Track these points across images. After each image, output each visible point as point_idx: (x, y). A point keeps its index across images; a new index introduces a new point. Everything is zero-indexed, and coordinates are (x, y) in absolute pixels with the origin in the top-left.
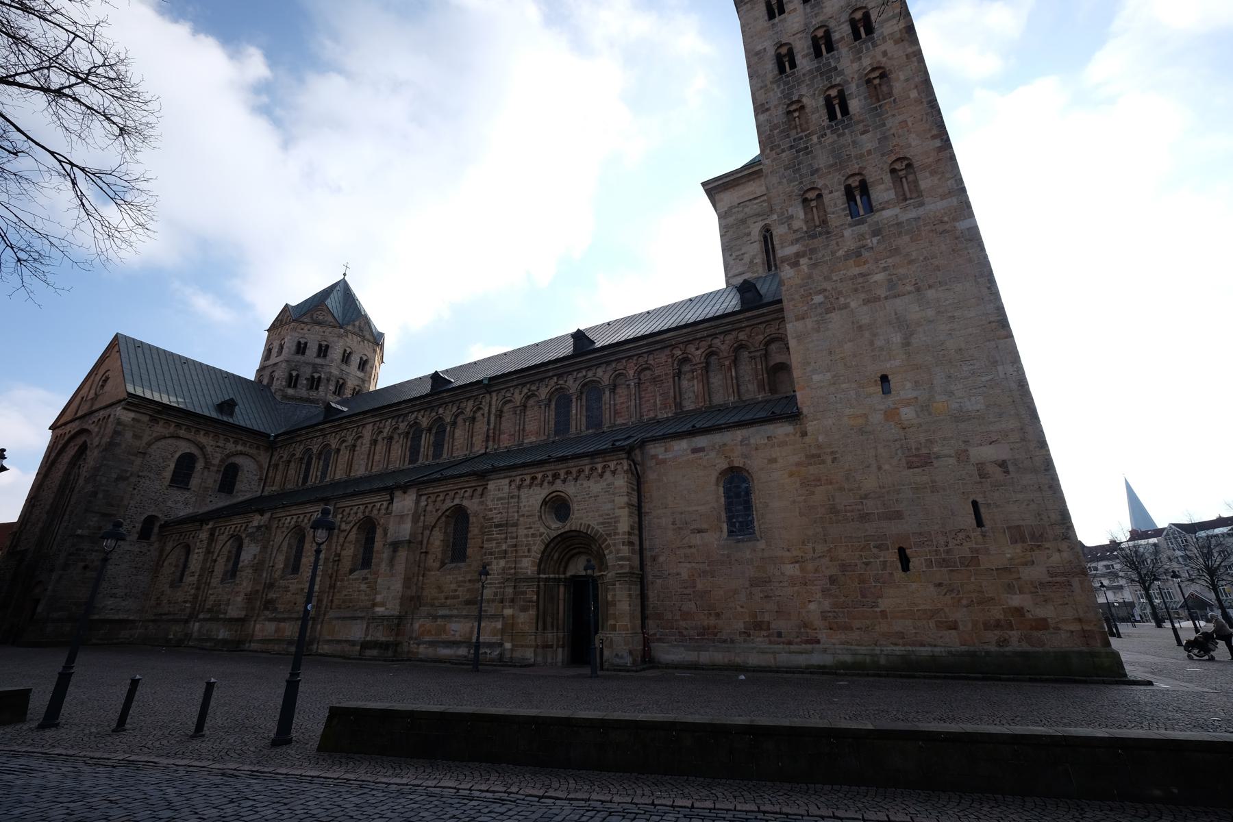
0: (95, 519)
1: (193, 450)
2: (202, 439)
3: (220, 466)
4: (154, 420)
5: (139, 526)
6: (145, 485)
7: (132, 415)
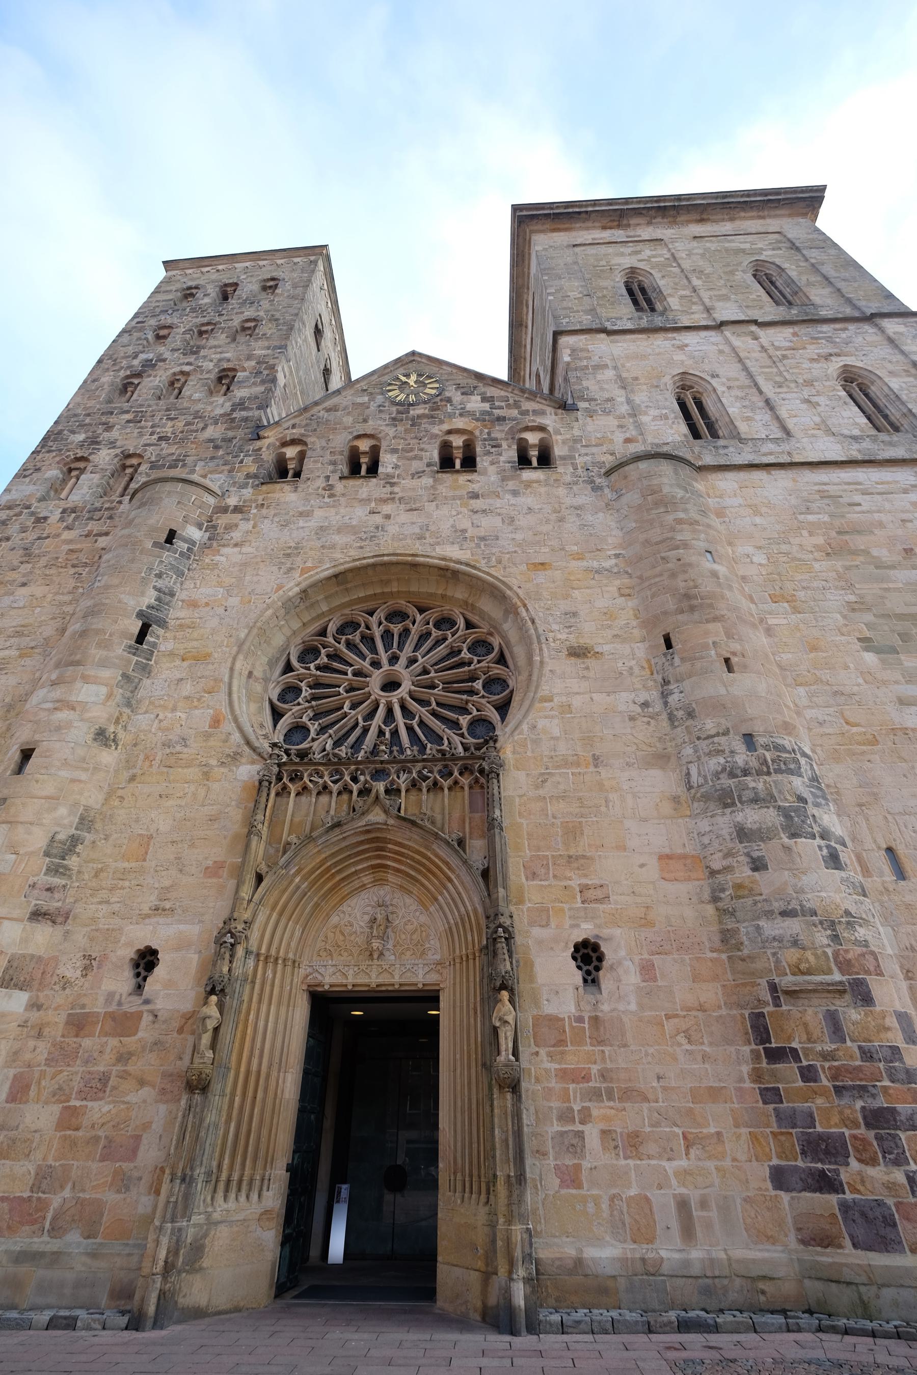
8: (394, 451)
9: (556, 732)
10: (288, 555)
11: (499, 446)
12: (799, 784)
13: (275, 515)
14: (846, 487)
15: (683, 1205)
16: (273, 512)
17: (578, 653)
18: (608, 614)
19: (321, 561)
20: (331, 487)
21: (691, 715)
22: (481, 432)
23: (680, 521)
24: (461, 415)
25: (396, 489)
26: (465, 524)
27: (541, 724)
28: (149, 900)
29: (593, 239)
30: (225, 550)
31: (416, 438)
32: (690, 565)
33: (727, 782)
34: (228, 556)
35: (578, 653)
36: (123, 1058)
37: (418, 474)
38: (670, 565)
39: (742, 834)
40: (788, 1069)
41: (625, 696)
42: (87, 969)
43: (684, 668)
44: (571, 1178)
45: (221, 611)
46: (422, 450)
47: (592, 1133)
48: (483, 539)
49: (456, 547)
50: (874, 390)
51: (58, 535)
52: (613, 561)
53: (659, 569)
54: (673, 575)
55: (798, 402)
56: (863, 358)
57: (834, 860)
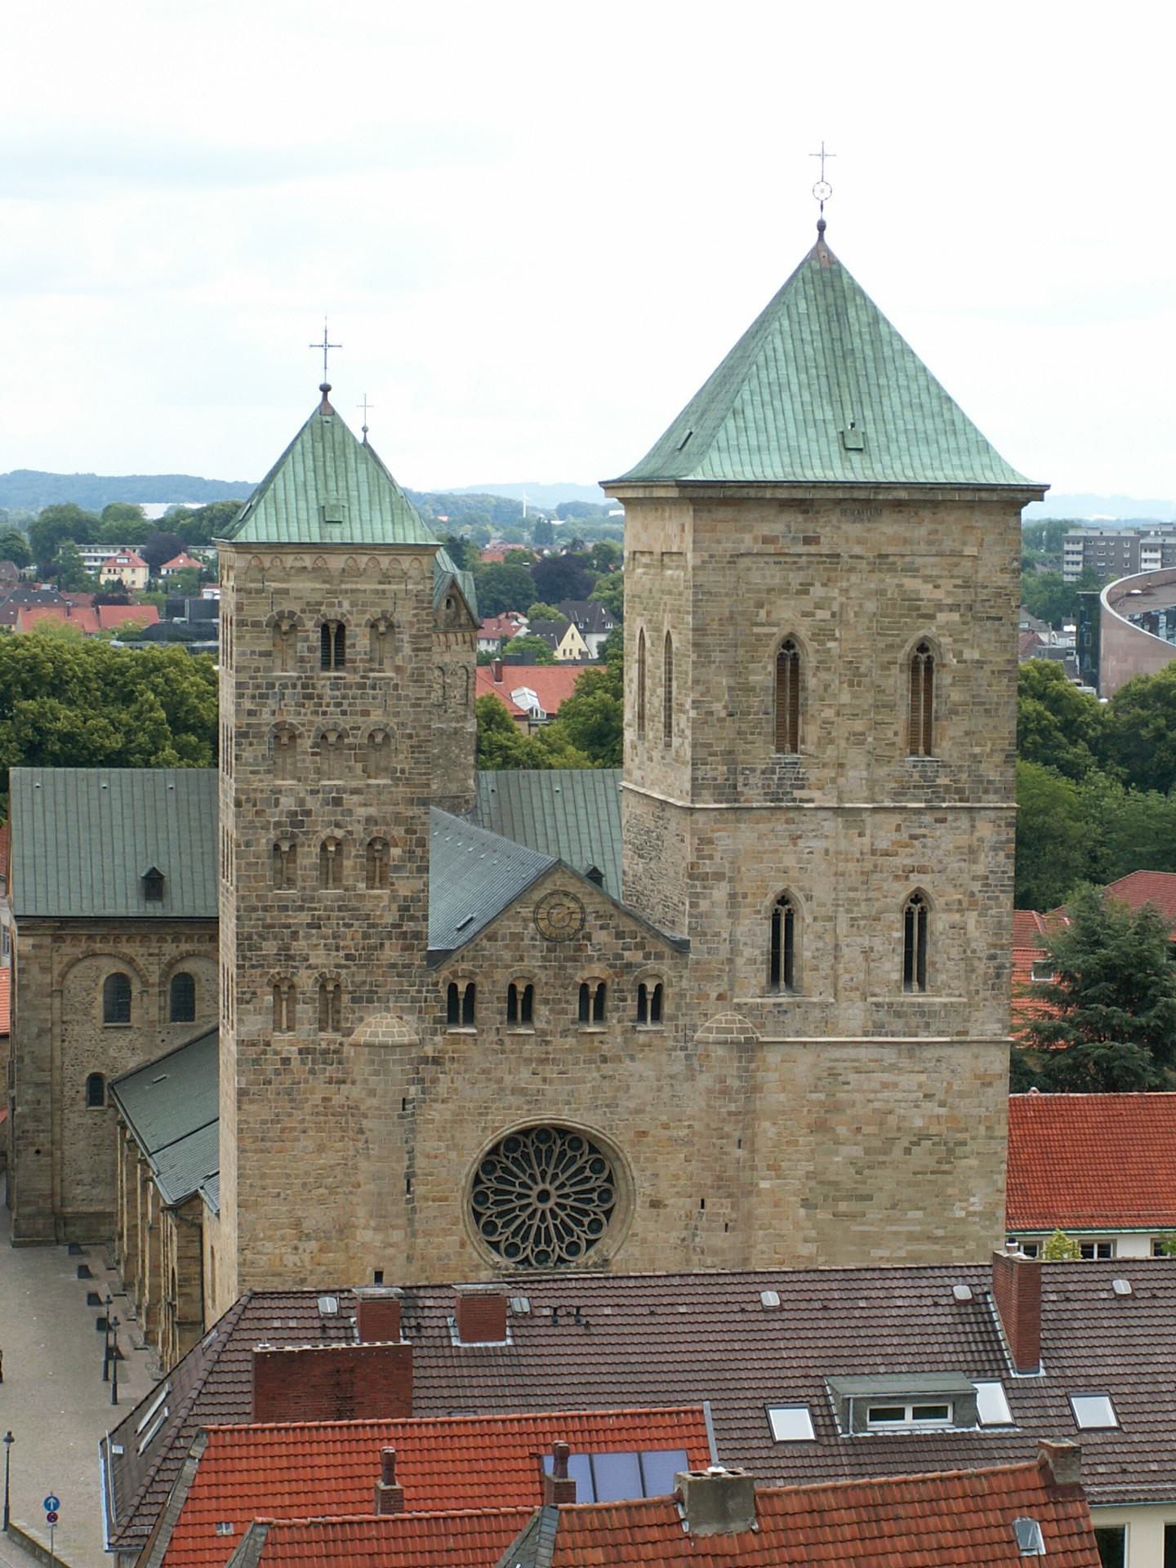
0: (31, 1091)
1: (123, 968)
2: (126, 948)
3: (161, 984)
4: (58, 939)
5: (83, 1090)
6: (75, 1032)
7: (30, 941)
8: (546, 1002)
10: (481, 1114)
11: (624, 1000)
13: (466, 1071)
16: (463, 1068)
17: (655, 1204)
18: (676, 1177)
19: (504, 1121)
20: (501, 1042)
21: (702, 1252)
22: (613, 981)
23: (730, 1113)
24: (599, 959)
25: (550, 1048)
29: (766, 540)
30: (436, 1106)
31: (562, 986)
34: (438, 1113)
35: (655, 1204)
37: (565, 1033)
41: (674, 1234)
45: (445, 1162)
46: (567, 1002)
50: (929, 916)
51: (306, 1081)
52: (686, 1131)
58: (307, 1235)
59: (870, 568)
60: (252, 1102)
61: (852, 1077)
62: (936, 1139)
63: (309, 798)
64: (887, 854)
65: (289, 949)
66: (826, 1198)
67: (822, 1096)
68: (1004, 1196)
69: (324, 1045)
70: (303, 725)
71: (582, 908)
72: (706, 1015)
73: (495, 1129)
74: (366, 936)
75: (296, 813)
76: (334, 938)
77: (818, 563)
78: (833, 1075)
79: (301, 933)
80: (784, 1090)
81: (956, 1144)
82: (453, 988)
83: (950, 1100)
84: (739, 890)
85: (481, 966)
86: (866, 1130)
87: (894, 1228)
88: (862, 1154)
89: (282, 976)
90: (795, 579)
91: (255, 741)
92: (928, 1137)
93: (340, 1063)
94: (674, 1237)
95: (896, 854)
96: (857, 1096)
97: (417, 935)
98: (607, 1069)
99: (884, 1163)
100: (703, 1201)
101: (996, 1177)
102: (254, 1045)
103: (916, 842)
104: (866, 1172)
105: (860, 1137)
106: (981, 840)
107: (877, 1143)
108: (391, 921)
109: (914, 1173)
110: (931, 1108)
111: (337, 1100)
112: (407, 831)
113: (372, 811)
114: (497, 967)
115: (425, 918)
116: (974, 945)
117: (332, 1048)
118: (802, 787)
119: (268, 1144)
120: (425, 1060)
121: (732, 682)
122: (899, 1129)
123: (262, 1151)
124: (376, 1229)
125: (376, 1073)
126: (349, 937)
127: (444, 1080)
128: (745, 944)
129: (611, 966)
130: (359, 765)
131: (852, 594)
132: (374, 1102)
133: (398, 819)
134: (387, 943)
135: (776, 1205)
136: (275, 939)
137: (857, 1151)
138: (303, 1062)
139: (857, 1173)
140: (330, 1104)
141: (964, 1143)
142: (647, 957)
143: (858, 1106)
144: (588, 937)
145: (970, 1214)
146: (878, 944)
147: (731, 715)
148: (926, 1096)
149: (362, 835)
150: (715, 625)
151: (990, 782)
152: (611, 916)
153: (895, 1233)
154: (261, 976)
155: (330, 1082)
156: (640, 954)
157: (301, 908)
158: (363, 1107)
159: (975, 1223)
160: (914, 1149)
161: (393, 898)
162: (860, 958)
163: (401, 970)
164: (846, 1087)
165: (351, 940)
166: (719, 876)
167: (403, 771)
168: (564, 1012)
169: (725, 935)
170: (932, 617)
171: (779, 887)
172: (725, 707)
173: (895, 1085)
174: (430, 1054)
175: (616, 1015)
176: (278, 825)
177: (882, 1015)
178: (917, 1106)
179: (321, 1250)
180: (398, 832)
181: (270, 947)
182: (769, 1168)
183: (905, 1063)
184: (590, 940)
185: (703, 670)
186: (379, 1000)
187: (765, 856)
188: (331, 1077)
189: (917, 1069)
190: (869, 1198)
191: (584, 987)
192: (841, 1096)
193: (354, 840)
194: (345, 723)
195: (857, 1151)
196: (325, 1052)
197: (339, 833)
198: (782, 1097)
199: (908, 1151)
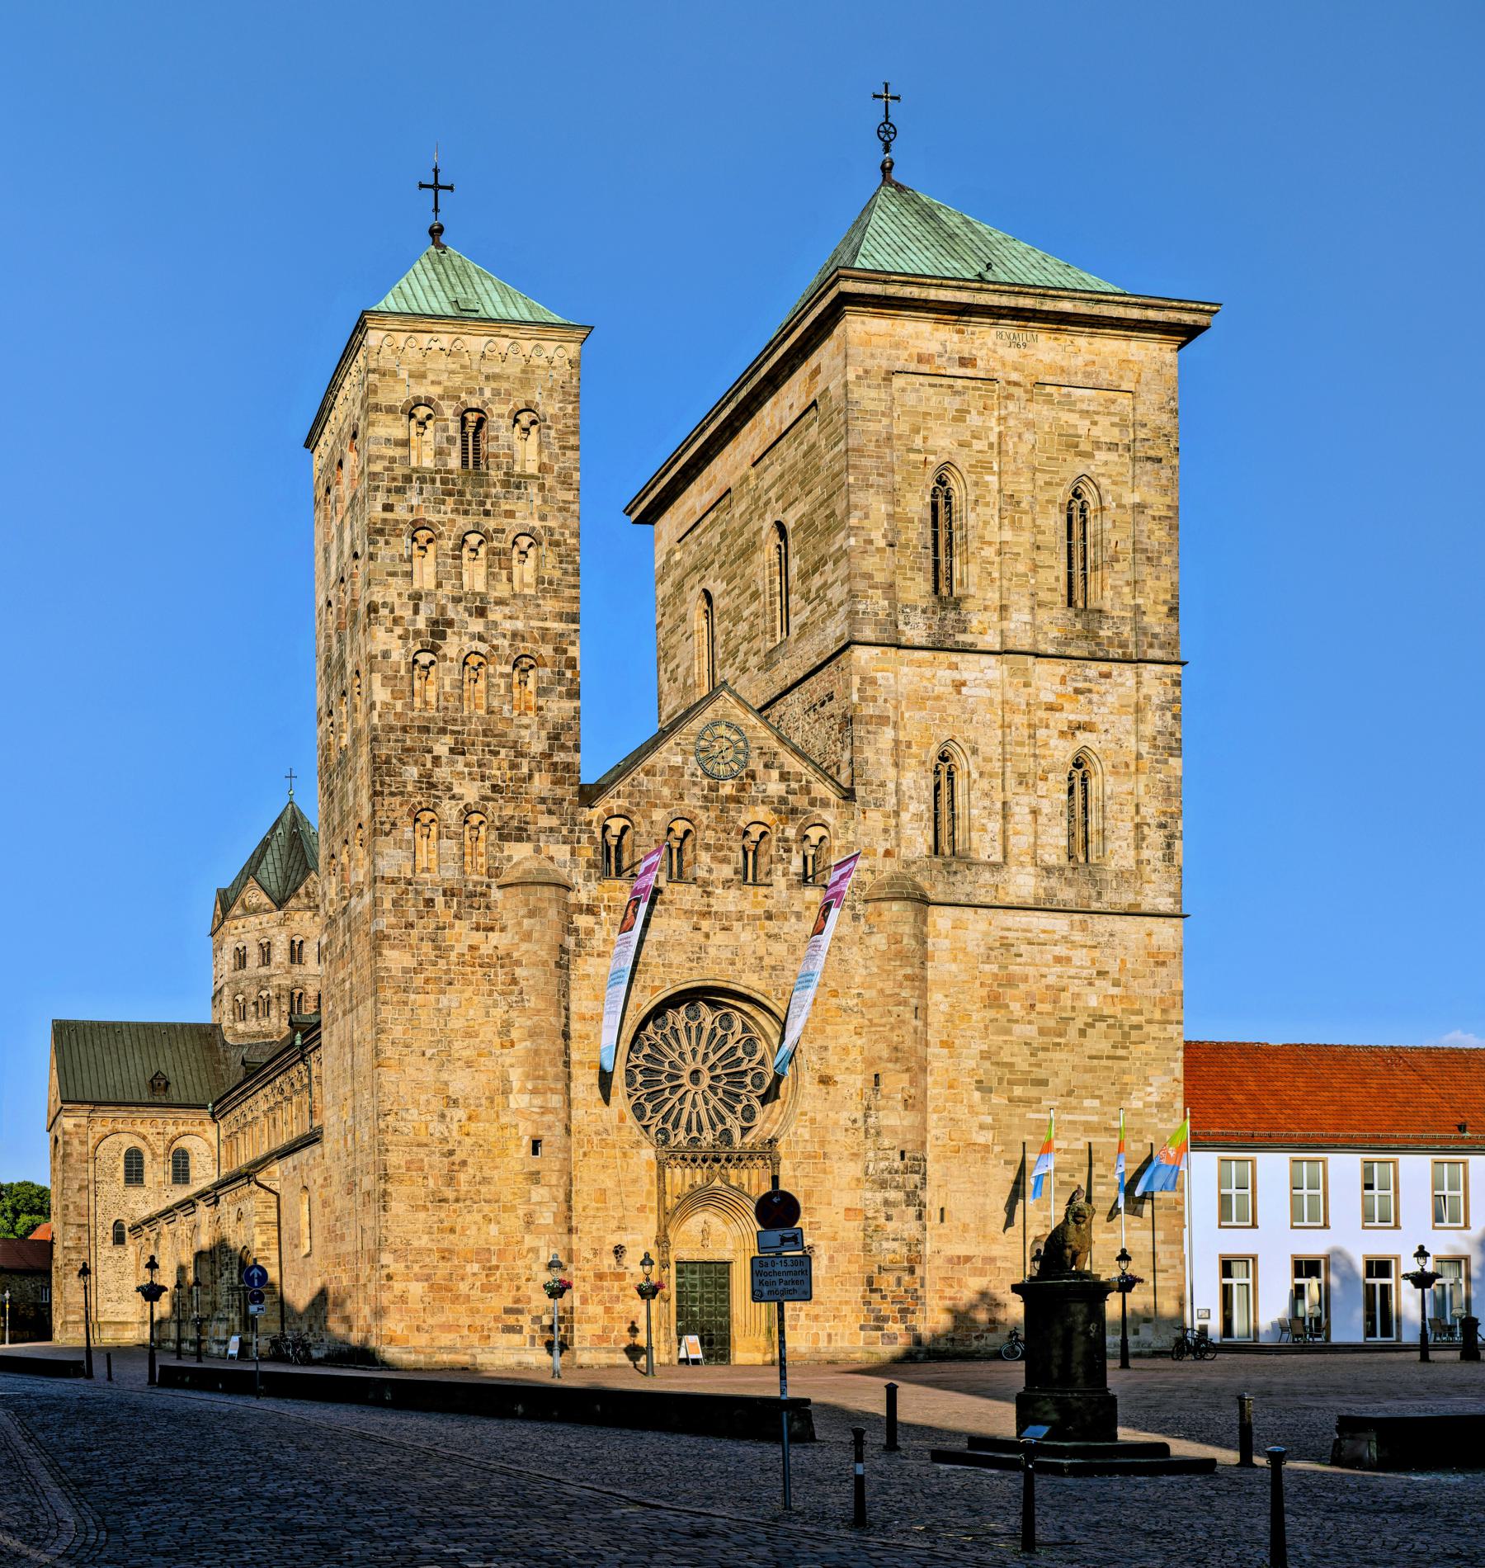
9: (807, 1137)
11: (788, 850)
12: (917, 1177)
14: (1020, 934)
15: (829, 1335)
17: (825, 1080)
18: (845, 1050)
23: (906, 977)
25: (712, 901)
26: (761, 952)
27: (800, 1131)
28: (614, 1224)
30: (591, 960)
31: (724, 831)
32: (903, 1022)
33: (886, 1176)
35: (825, 1080)
36: (622, 1289)
37: (727, 884)
38: (892, 1020)
39: (886, 1203)
40: (876, 1297)
41: (845, 1114)
42: (595, 1254)
43: (882, 1103)
44: (794, 1328)
46: (730, 849)
47: (802, 1314)
48: (774, 968)
49: (756, 976)
51: (452, 926)
52: (855, 1001)
53: (884, 1020)
54: (892, 1029)
55: (1027, 810)
56: (1103, 737)
57: (920, 1217)
58: (455, 1101)
59: (1028, 396)
60: (393, 947)
61: (1024, 948)
62: (1111, 1021)
63: (450, 606)
64: (1051, 708)
65: (431, 776)
66: (1000, 1080)
67: (994, 968)
68: (1181, 1087)
69: (470, 887)
70: (443, 524)
71: (745, 740)
72: (873, 872)
73: (655, 989)
74: (514, 766)
75: (435, 623)
76: (480, 766)
77: (974, 389)
78: (1007, 946)
79: (444, 760)
80: (955, 960)
81: (1133, 1027)
82: (605, 828)
83: (1123, 979)
84: (902, 736)
85: (638, 804)
86: (1039, 1007)
87: (1070, 1117)
88: (1035, 1033)
89: (424, 805)
90: (955, 403)
91: (392, 540)
92: (1102, 1018)
93: (488, 907)
94: (844, 1118)
95: (1062, 709)
96: (1031, 971)
97: (568, 767)
98: (772, 926)
99: (1059, 1044)
100: (877, 1076)
101: (1173, 1065)
102: (393, 882)
103: (1081, 697)
104: (1041, 1054)
105: (1034, 1015)
106: (1148, 698)
107: (1052, 1023)
108: (540, 750)
109: (1090, 1057)
110: (1102, 984)
111: (485, 950)
112: (556, 650)
113: (519, 625)
114: (656, 806)
115: (577, 748)
116: (1142, 809)
117: (478, 889)
118: (964, 631)
119: (412, 996)
120: (580, 909)
121: (890, 509)
122: (1073, 1008)
123: (405, 1003)
124: (534, 1092)
125: (532, 914)
126: (495, 765)
127: (600, 934)
128: (911, 798)
129: (775, 810)
130: (504, 573)
131: (1012, 422)
132: (524, 946)
133: (545, 635)
134: (537, 775)
135: (951, 1087)
136: (416, 763)
137: (1031, 1031)
138: (447, 905)
139: (1032, 1055)
140: (477, 954)
141: (1139, 1027)
142: (812, 803)
143: (1031, 980)
144: (752, 776)
145: (1147, 1105)
146: (1046, 807)
147: (891, 545)
148: (1099, 973)
149: (508, 652)
150: (872, 446)
151: (1155, 636)
152: (776, 754)
153: (1070, 1122)
154: (401, 805)
155: (478, 929)
156: (805, 799)
157: (443, 731)
158: (515, 955)
159: (1151, 1115)
160: (1089, 1031)
161: (542, 725)
162: (1029, 817)
163: (553, 805)
164: (1019, 960)
165: (498, 770)
166: (883, 720)
167: (551, 583)
168: (725, 860)
169: (891, 786)
170: (1090, 455)
171: (946, 735)
172: (885, 536)
173: (1068, 960)
174: (585, 901)
175: (780, 867)
176: (418, 633)
177: (1053, 882)
178: (1091, 984)
179: (469, 1118)
180: (547, 650)
181: (412, 772)
182: (944, 1044)
183: (1077, 937)
184: (753, 778)
185: (861, 494)
186: (529, 839)
187: (929, 703)
188: (478, 924)
189: (1089, 943)
190: (1043, 1083)
191: (746, 833)
192: (1014, 969)
193: (500, 656)
194: (490, 524)
195: (1031, 1031)
196: (472, 895)
197: (483, 648)
198: (954, 967)
199: (1082, 1033)
